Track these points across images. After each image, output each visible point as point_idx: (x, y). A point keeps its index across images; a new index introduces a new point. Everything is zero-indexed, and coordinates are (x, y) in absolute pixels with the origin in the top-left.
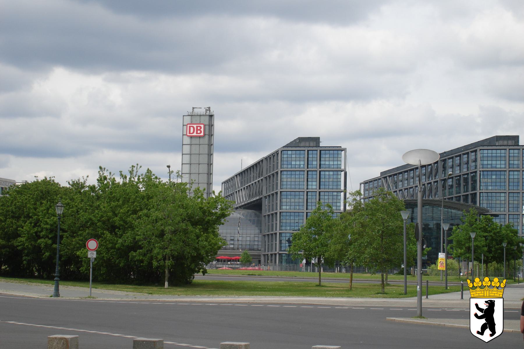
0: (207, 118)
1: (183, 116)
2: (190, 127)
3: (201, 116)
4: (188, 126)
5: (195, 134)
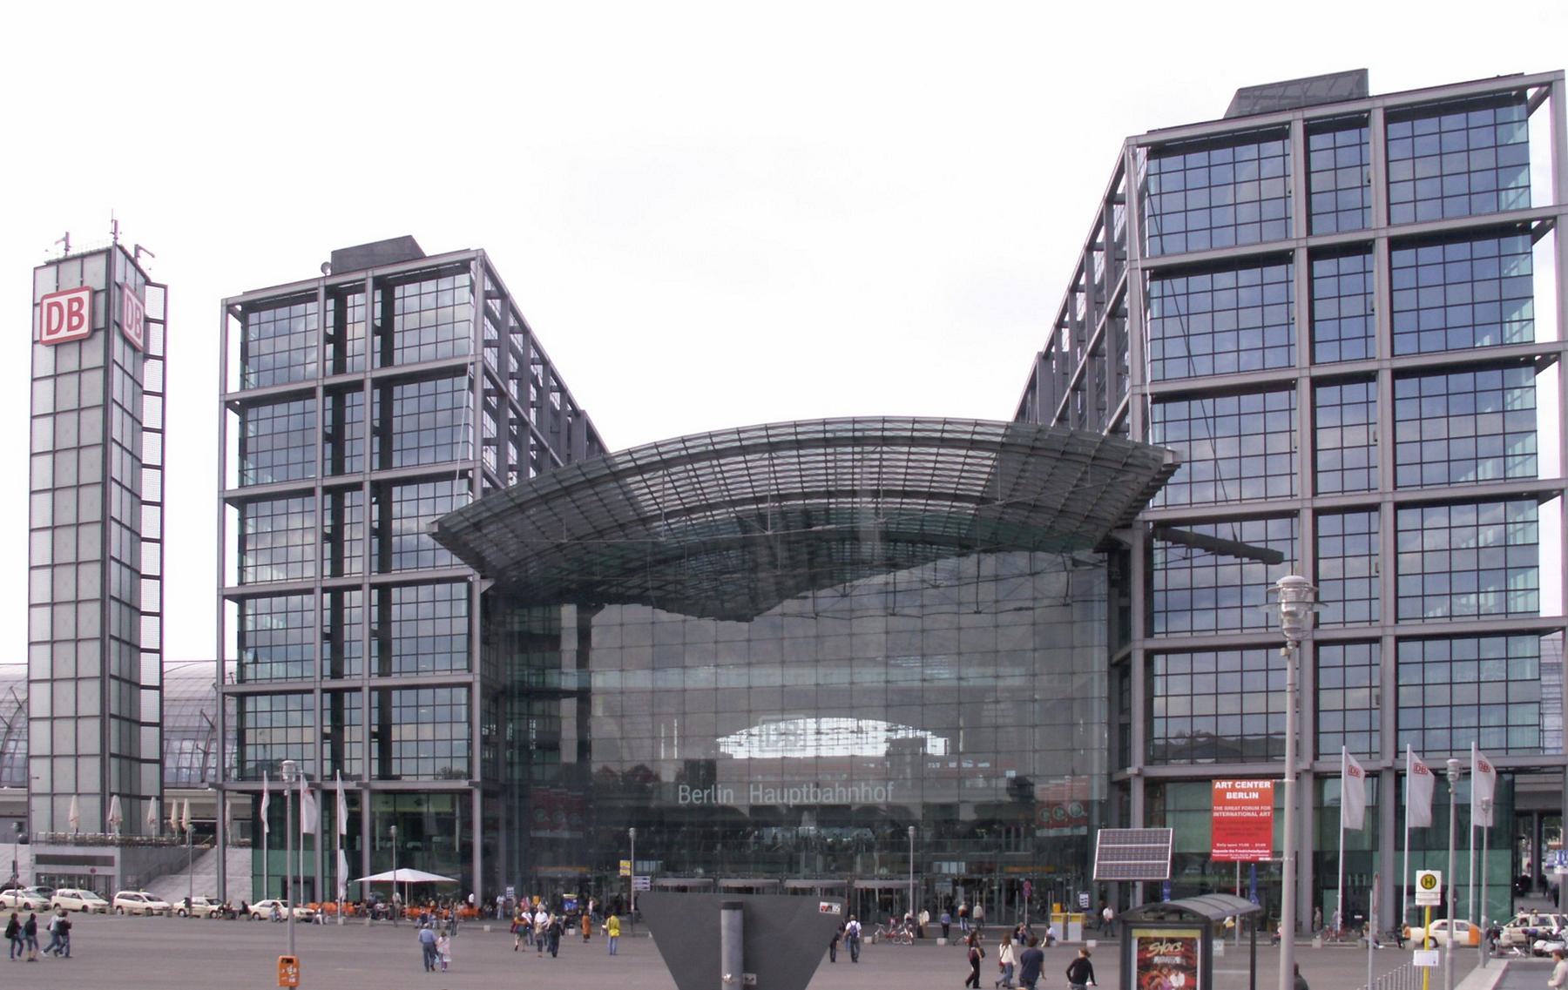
0: (101, 262)
1: (36, 269)
2: (50, 306)
3: (85, 260)
4: (46, 302)
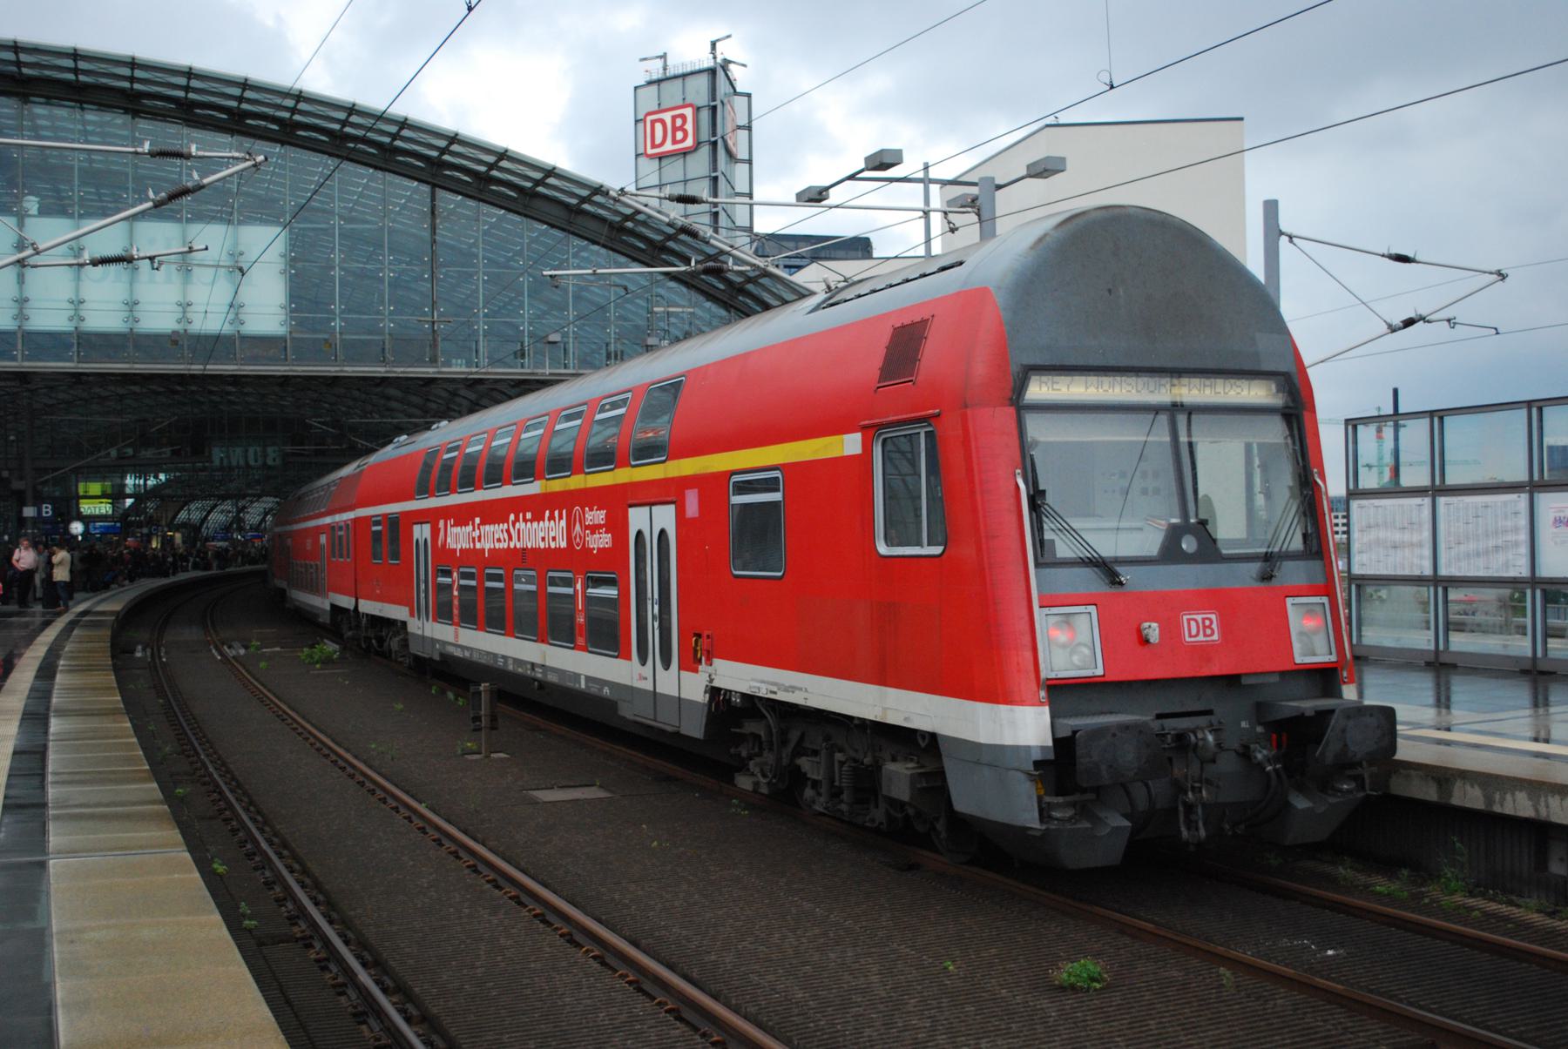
0: (704, 80)
1: (636, 88)
2: (653, 122)
4: (650, 118)
5: (668, 146)
